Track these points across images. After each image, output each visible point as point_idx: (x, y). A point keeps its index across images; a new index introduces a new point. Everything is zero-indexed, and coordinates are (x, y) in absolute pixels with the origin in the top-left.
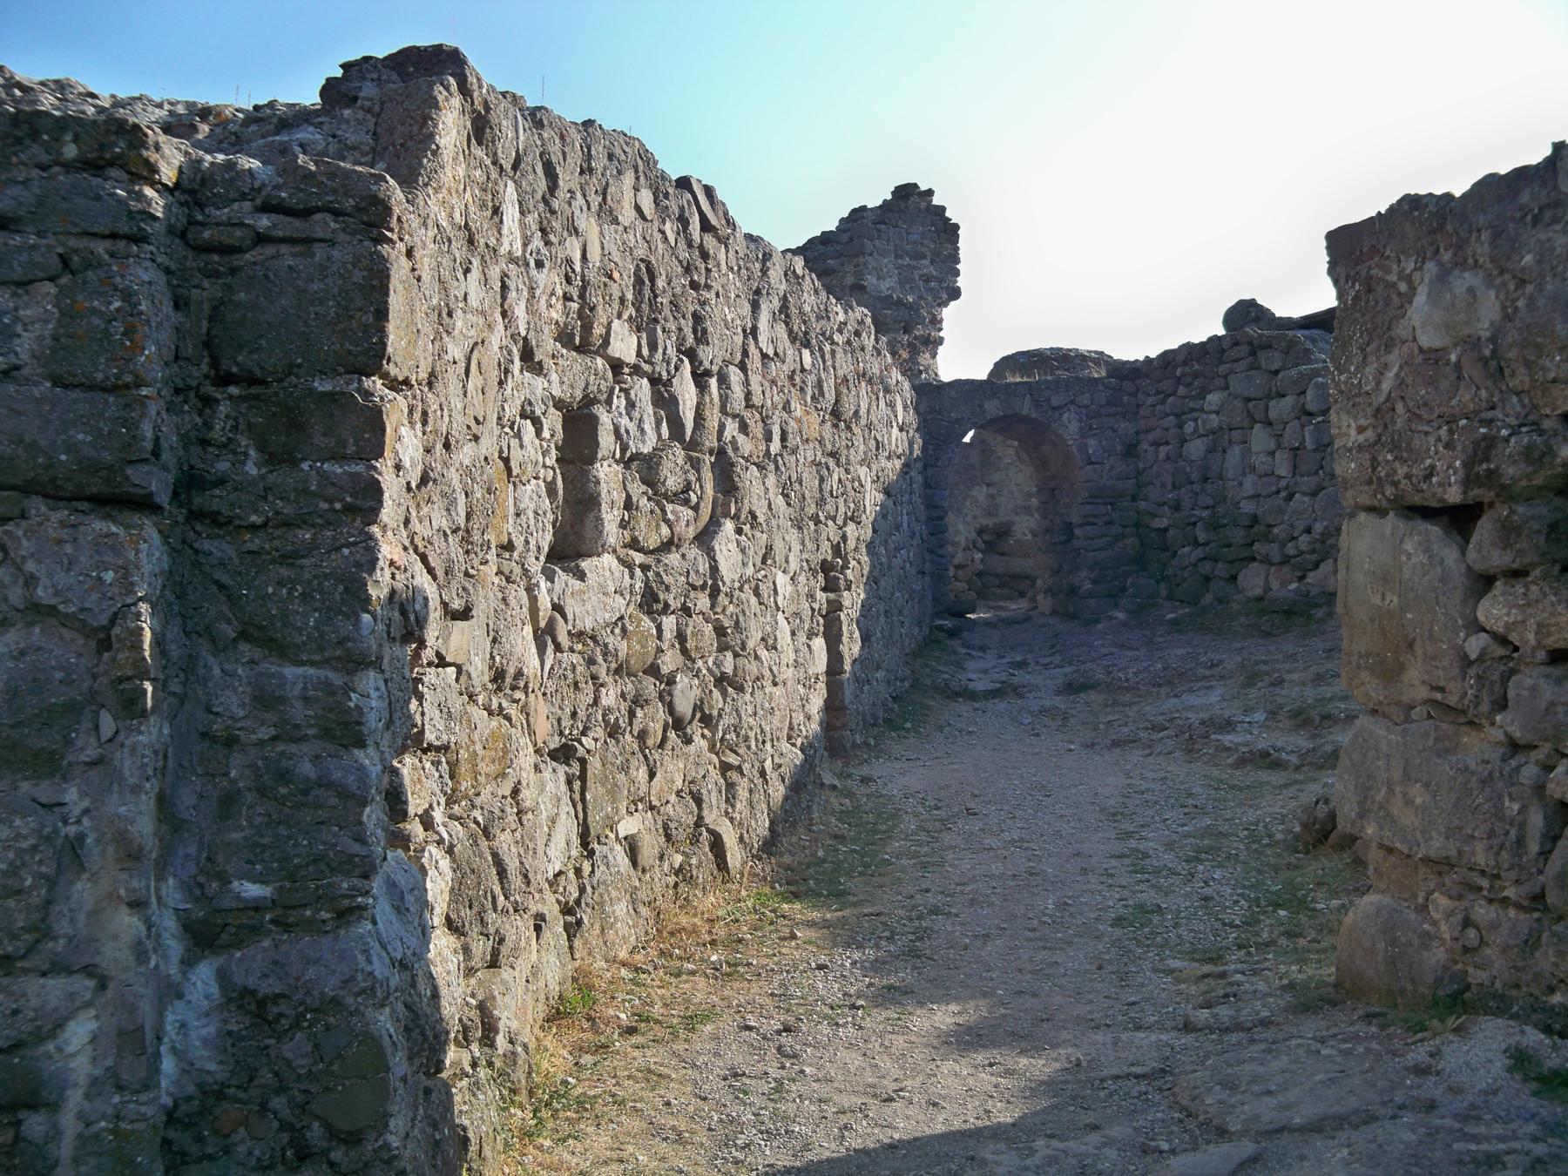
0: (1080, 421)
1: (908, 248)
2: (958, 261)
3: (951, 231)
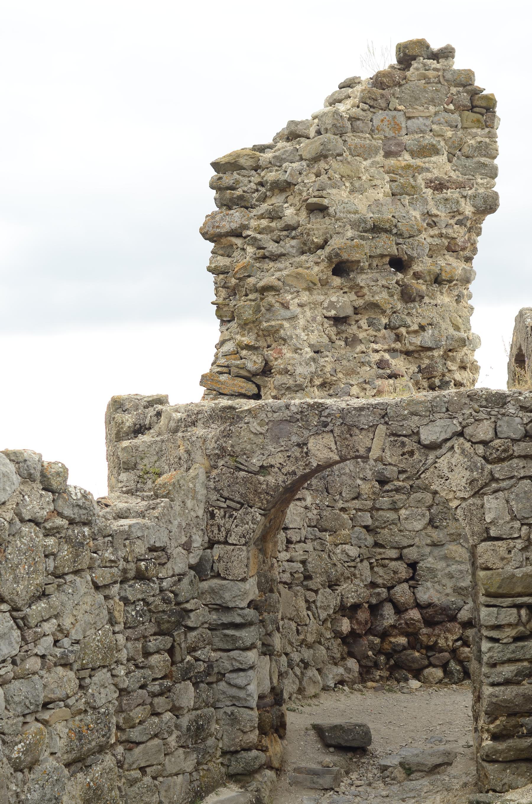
1: (406, 140)
3: (481, 108)
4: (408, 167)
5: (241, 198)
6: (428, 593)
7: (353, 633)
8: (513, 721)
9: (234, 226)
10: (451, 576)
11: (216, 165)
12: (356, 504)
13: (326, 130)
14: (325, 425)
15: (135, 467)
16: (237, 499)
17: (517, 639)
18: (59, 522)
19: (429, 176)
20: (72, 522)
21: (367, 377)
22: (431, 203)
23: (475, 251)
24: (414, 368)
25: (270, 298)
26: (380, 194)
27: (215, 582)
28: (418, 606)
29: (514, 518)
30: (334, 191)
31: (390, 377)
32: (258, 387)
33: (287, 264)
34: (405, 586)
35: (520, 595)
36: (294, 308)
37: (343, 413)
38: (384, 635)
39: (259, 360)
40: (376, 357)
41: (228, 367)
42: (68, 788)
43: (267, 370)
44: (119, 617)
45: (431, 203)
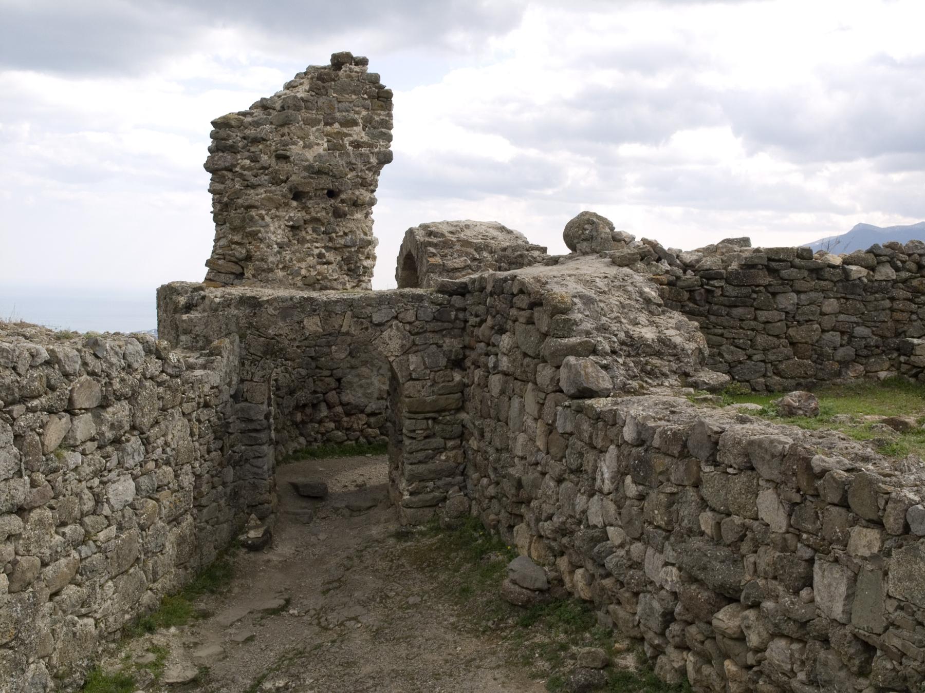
0: (404, 338)
1: (338, 115)
2: (390, 127)
4: (339, 133)
5: (232, 146)
6: (347, 397)
7: (303, 422)
8: (422, 484)
9: (227, 164)
10: (361, 386)
11: (214, 123)
12: (306, 343)
13: (288, 107)
14: (315, 310)
15: (190, 332)
16: (259, 354)
17: (426, 438)
18: (165, 377)
19: (351, 139)
20: (171, 376)
23: (376, 186)
24: (339, 258)
25: (253, 213)
26: (322, 147)
27: (243, 404)
28: (341, 404)
29: (426, 368)
30: (293, 147)
31: (325, 264)
32: (243, 268)
33: (262, 191)
34: (334, 392)
35: (429, 412)
36: (267, 219)
37: (327, 304)
38: (320, 422)
39: (244, 251)
40: (316, 251)
42: (169, 537)
43: (249, 258)
44: (196, 431)
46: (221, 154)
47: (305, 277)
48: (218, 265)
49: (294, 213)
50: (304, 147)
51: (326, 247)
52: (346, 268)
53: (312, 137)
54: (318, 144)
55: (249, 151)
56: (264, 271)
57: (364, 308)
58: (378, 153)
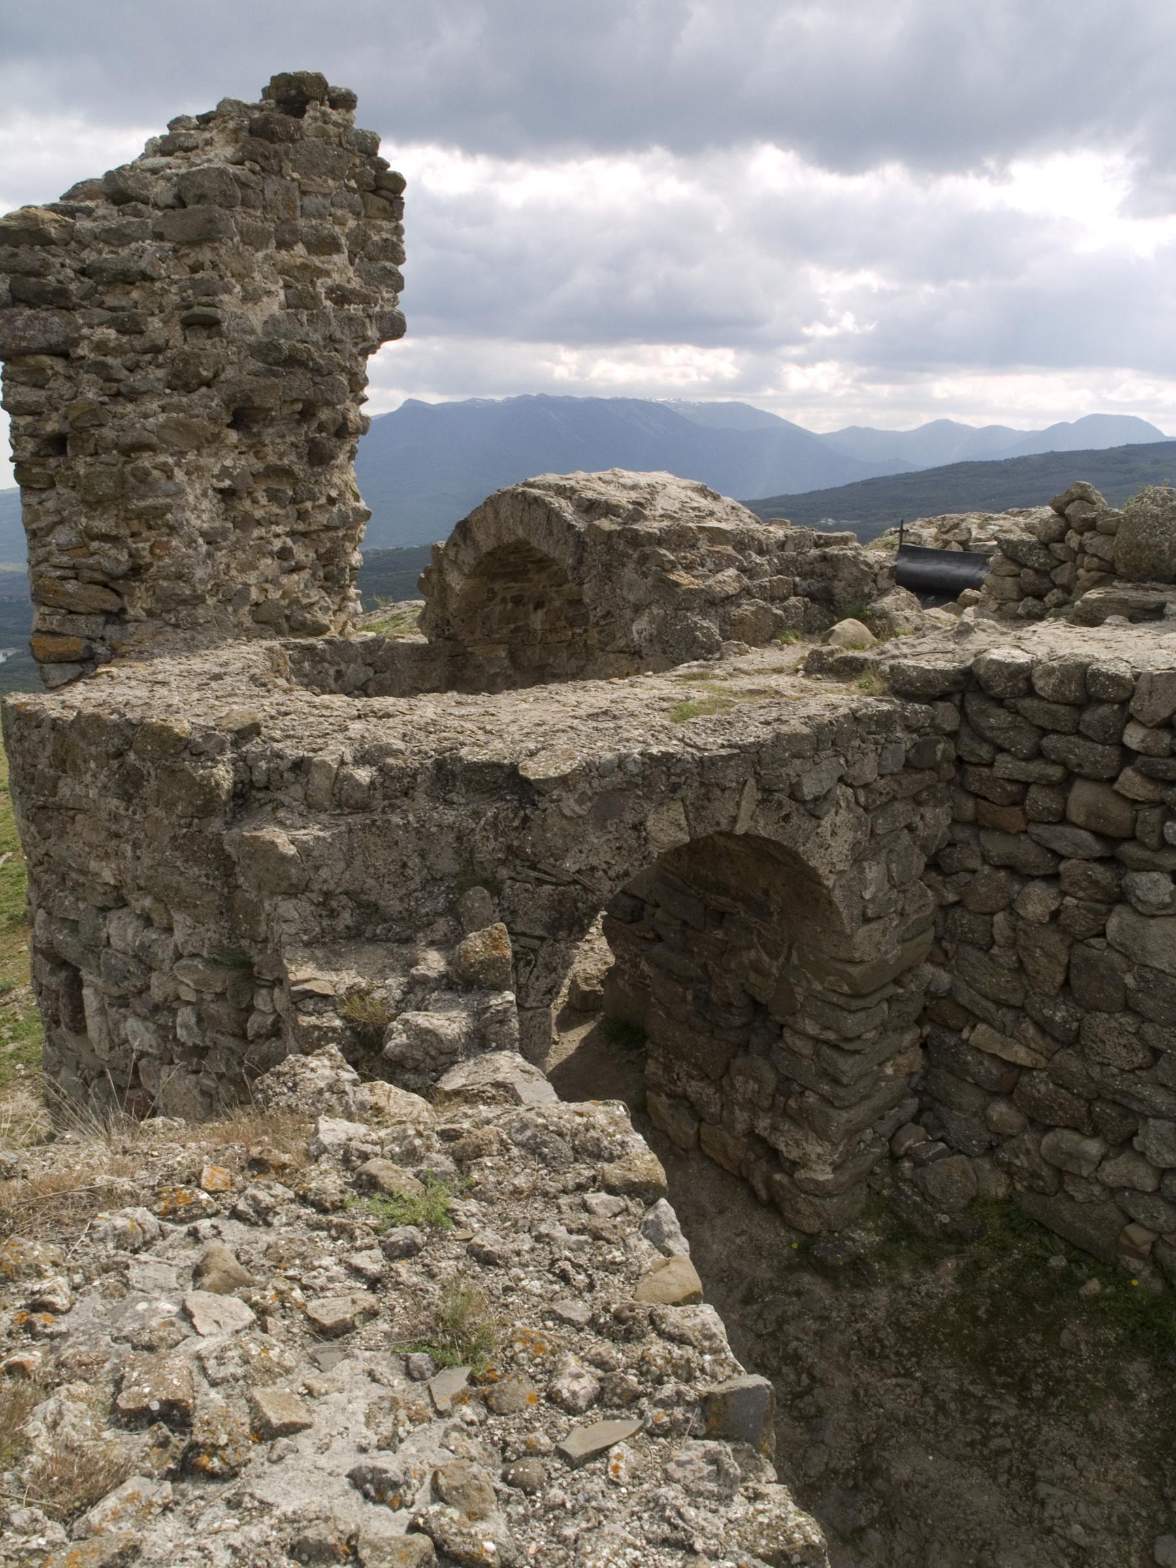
1: (301, 223)
2: (399, 258)
4: (304, 267)
9: (54, 339)
14: (675, 788)
15: (307, 888)
16: (539, 932)
19: (330, 282)
21: (270, 574)
22: (334, 322)
25: (145, 461)
26: (273, 306)
29: (894, 886)
30: (225, 297)
33: (155, 406)
39: (124, 557)
40: (277, 544)
41: (73, 567)
43: (136, 571)
45: (334, 322)
46: (28, 312)
47: (257, 604)
48: (66, 593)
49: (231, 459)
50: (244, 300)
51: (292, 534)
52: (321, 574)
53: (257, 276)
54: (269, 293)
55: (101, 305)
56: (184, 602)
57: (784, 763)
58: (381, 317)
